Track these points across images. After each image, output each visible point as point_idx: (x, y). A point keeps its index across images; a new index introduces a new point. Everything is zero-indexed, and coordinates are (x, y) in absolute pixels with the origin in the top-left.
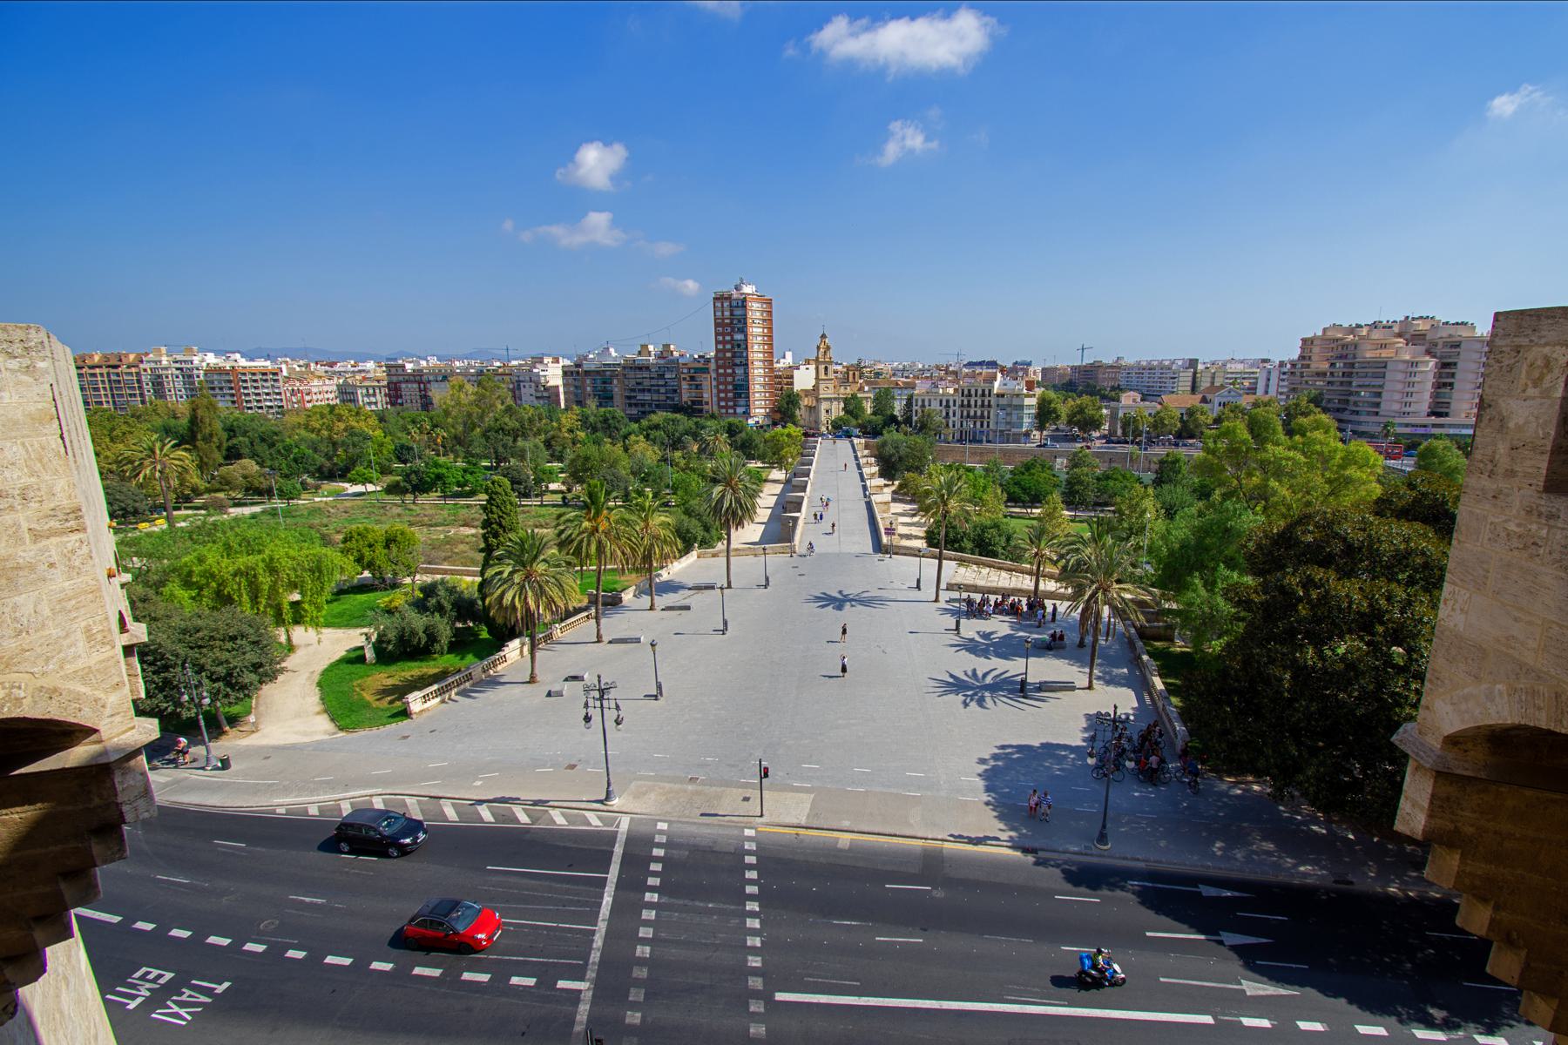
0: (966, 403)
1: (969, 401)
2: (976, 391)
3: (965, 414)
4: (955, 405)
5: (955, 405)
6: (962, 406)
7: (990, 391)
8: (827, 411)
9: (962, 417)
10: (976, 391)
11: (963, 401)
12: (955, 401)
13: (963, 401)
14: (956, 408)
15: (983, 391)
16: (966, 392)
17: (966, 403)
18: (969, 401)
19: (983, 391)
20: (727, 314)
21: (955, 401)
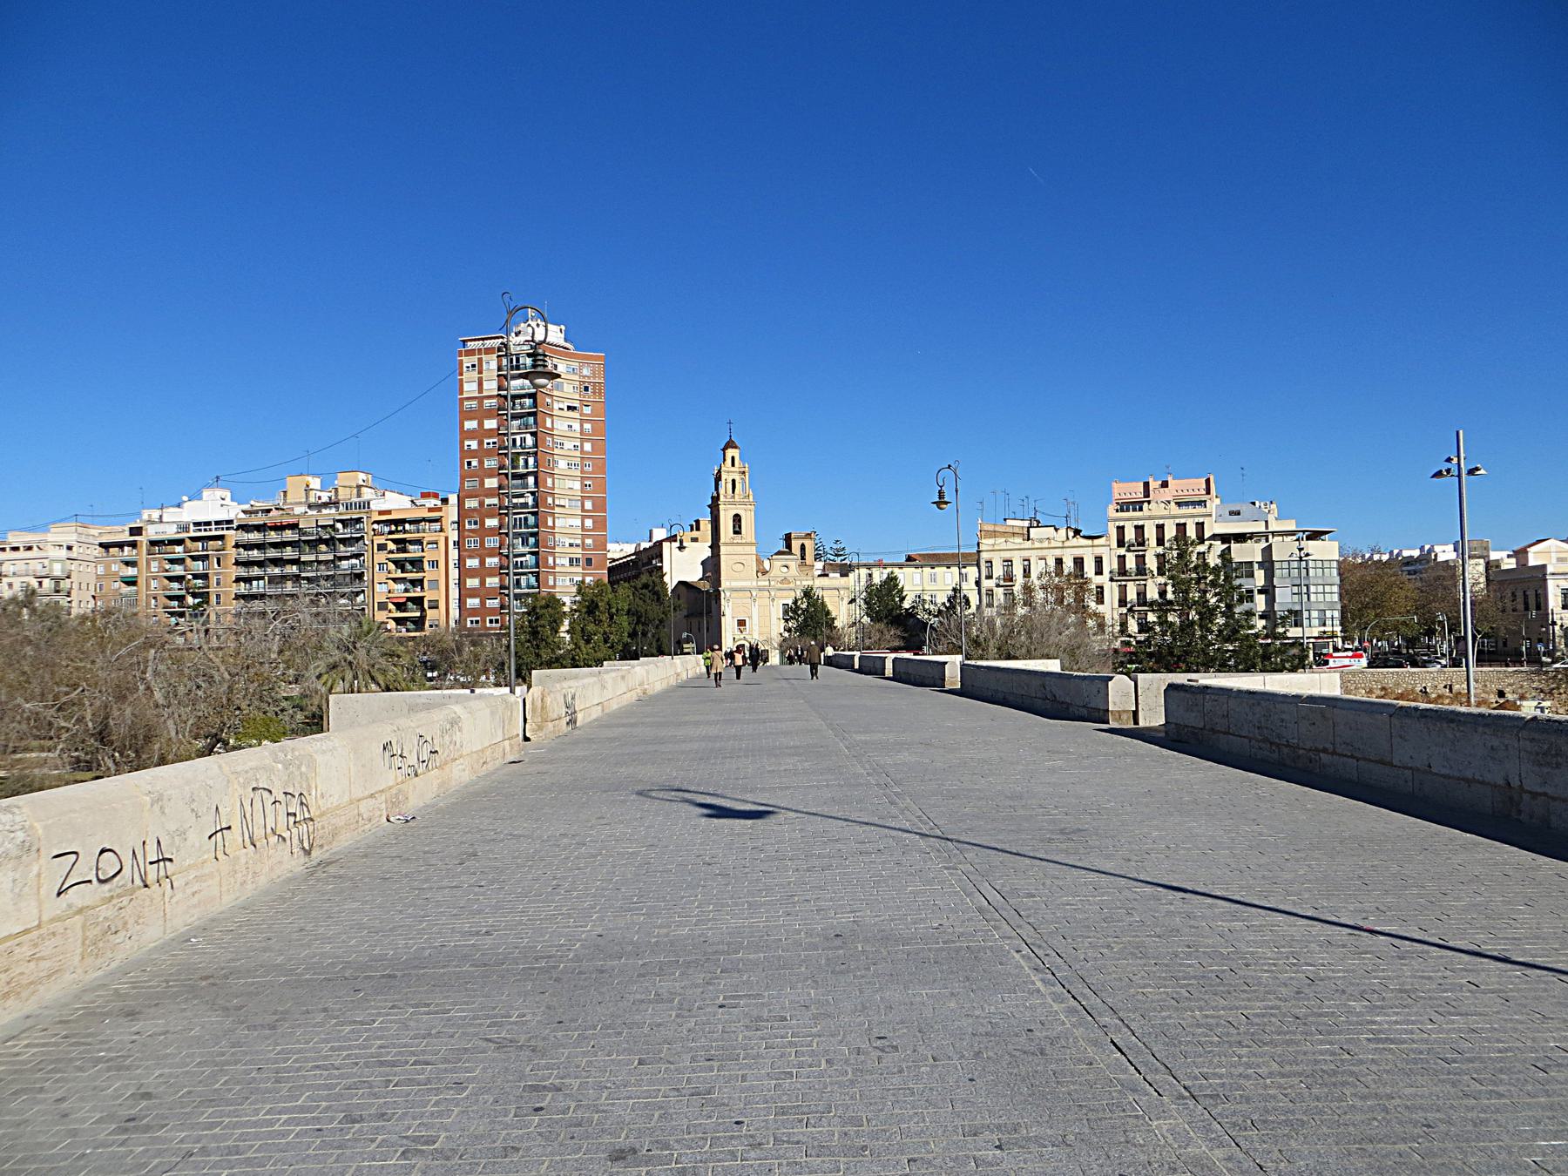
0: (1131, 563)
1: (1141, 560)
2: (1160, 528)
3: (1132, 595)
4: (1099, 572)
5: (1099, 572)
6: (1123, 571)
7: (1200, 526)
8: (742, 623)
9: (1123, 602)
10: (1160, 528)
11: (1122, 559)
12: (1099, 561)
13: (1122, 559)
14: (1103, 579)
15: (1181, 527)
16: (1130, 535)
17: (1131, 563)
18: (1141, 560)
19: (1181, 527)
20: (491, 386)
21: (1099, 561)
